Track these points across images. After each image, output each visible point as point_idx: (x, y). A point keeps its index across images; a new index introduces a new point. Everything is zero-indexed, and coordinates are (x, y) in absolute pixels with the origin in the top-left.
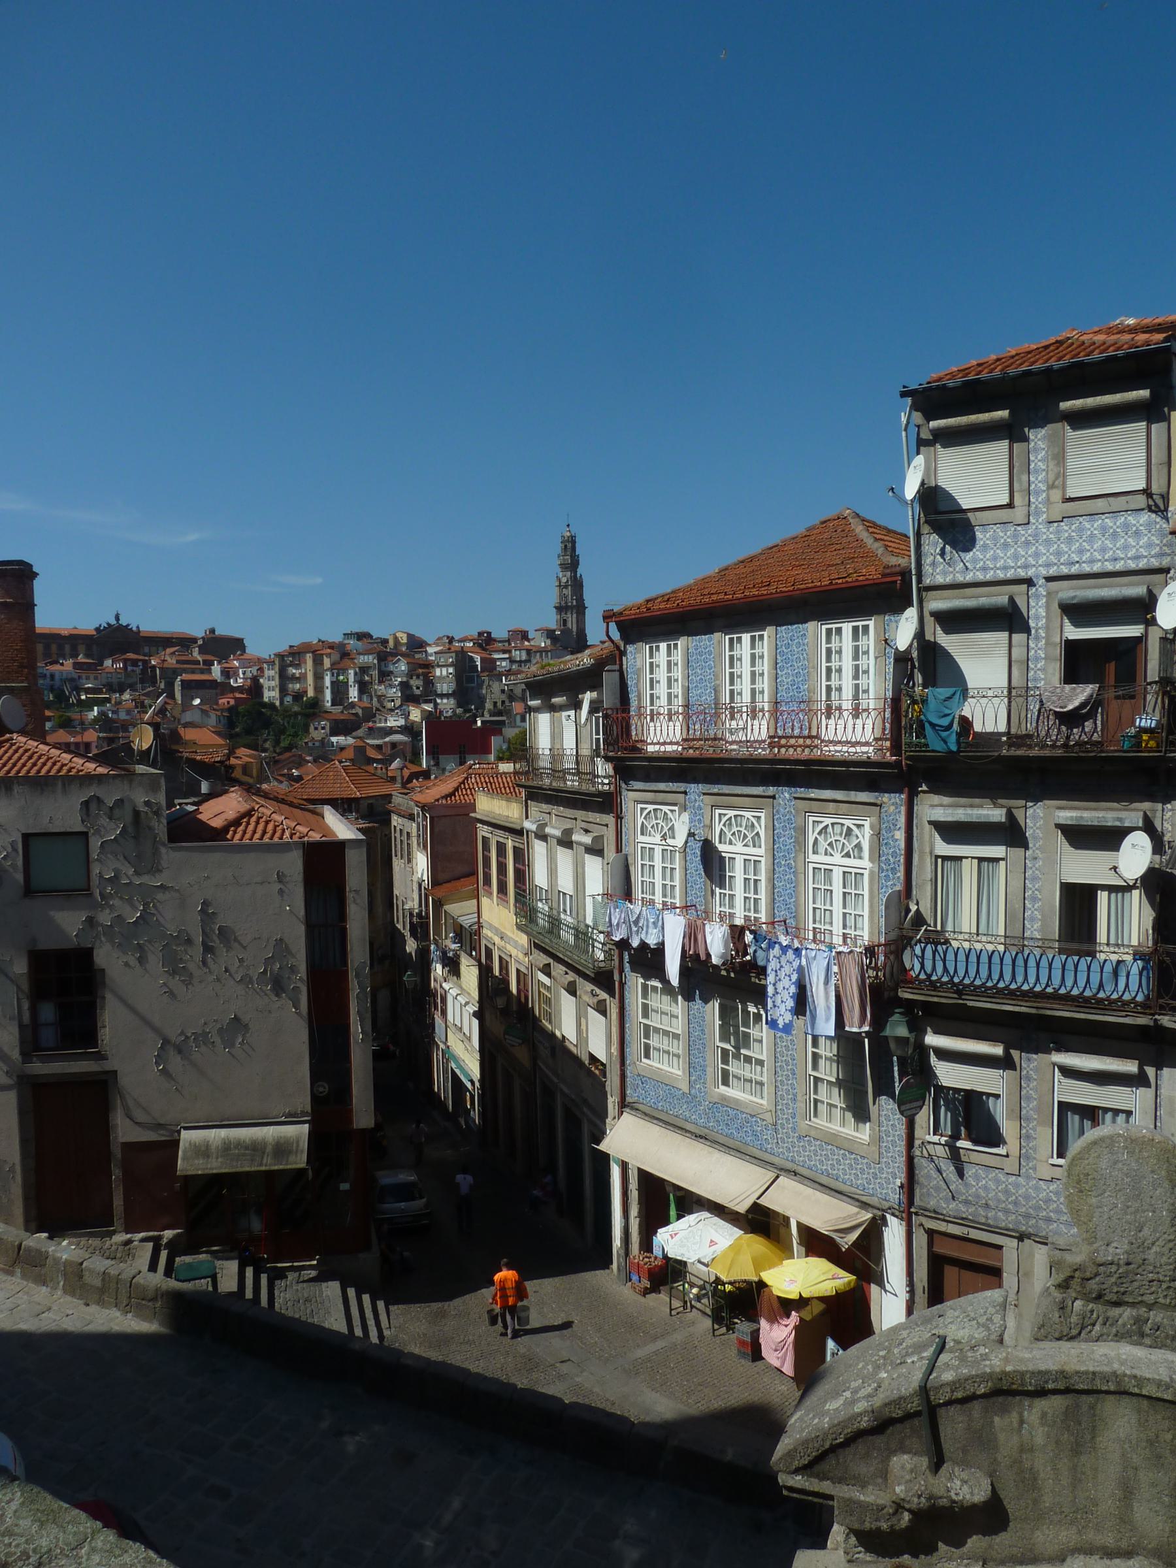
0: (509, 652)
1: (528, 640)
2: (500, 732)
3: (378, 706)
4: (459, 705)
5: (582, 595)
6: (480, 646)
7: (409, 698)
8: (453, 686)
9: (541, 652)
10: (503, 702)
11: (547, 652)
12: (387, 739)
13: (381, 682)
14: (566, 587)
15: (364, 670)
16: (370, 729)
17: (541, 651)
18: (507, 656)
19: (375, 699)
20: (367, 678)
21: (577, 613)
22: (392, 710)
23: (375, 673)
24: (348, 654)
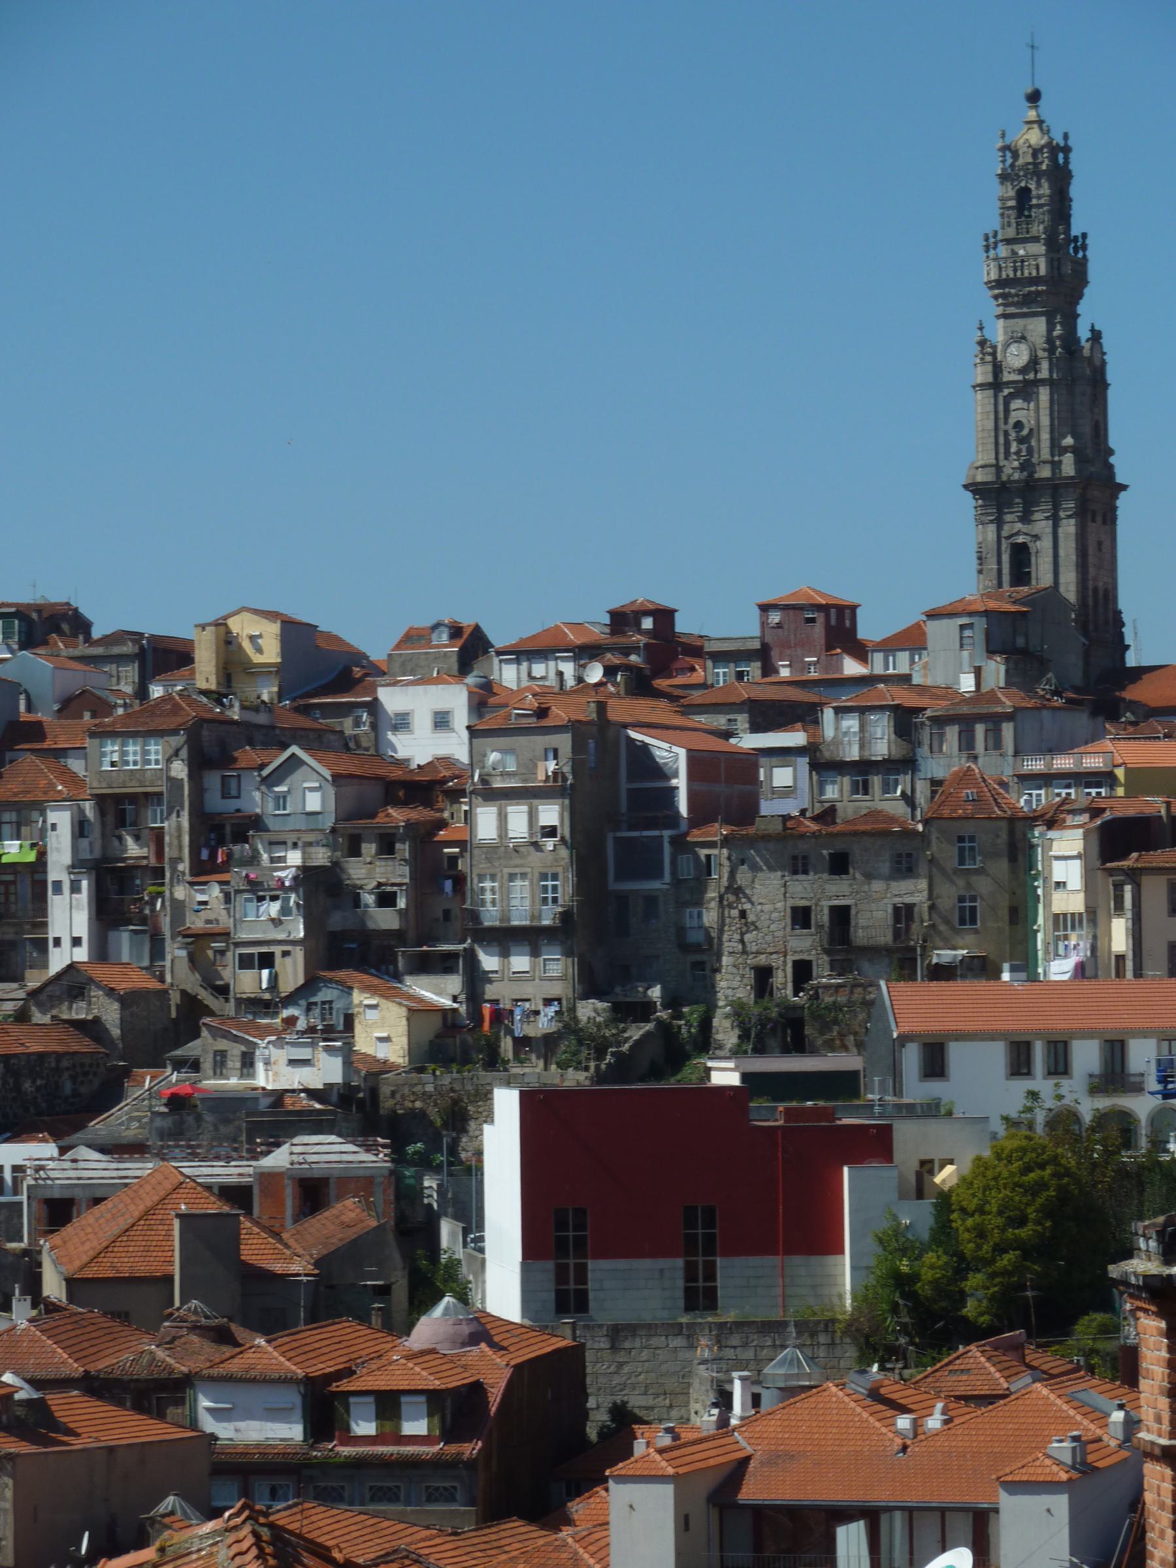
0: (803, 714)
1: (860, 651)
2: (875, 1144)
3: (191, 982)
4: (590, 987)
5: (1100, 429)
6: (640, 685)
7: (347, 948)
8: (565, 890)
9: (966, 723)
10: (802, 971)
11: (994, 721)
12: (279, 1159)
13: (203, 869)
14: (1026, 390)
15: (120, 809)
16: (178, 1103)
17: (968, 718)
18: (795, 738)
19: (176, 952)
20: (133, 849)
21: (1083, 514)
22: (262, 1006)
23: (178, 827)
24: (36, 731)
